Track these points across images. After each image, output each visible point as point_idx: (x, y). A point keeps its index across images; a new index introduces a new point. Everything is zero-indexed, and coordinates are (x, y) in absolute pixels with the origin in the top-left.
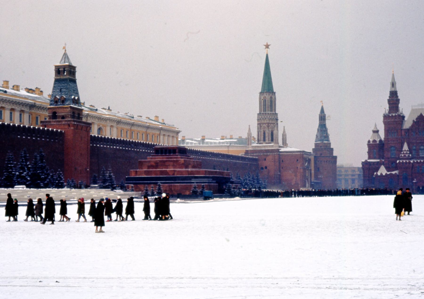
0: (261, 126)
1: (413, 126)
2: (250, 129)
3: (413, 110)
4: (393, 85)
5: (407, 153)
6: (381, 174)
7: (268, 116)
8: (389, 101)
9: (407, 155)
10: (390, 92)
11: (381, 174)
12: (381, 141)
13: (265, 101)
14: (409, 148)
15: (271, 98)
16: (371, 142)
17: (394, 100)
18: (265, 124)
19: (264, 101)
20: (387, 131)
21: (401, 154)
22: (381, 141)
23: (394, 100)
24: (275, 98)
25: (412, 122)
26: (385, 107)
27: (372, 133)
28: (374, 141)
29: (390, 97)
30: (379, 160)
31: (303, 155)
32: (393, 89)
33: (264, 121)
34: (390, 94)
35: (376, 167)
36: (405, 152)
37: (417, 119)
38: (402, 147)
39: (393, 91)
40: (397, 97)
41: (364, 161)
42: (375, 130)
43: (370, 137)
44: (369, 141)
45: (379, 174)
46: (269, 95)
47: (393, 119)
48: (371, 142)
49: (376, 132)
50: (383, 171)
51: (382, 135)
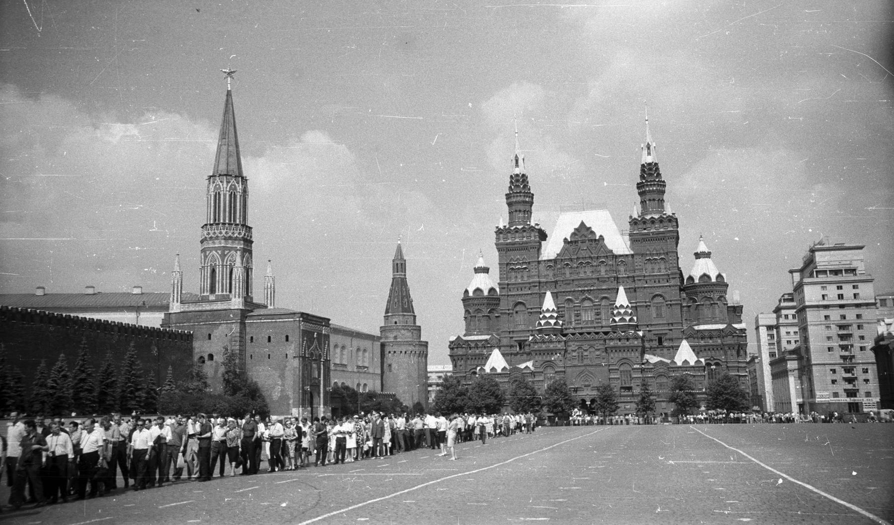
0: (206, 256)
1: (564, 250)
5: (551, 317)
6: (493, 369)
7: (224, 232)
9: (552, 321)
11: (493, 369)
13: (217, 196)
15: (233, 190)
16: (471, 294)
18: (216, 249)
19: (215, 196)
20: (506, 267)
22: (492, 290)
23: (520, 194)
24: (245, 191)
25: (562, 244)
33: (214, 243)
34: (511, 182)
35: (480, 353)
36: (548, 315)
37: (573, 234)
38: (541, 303)
41: (453, 338)
45: (487, 369)
46: (228, 182)
48: (471, 294)
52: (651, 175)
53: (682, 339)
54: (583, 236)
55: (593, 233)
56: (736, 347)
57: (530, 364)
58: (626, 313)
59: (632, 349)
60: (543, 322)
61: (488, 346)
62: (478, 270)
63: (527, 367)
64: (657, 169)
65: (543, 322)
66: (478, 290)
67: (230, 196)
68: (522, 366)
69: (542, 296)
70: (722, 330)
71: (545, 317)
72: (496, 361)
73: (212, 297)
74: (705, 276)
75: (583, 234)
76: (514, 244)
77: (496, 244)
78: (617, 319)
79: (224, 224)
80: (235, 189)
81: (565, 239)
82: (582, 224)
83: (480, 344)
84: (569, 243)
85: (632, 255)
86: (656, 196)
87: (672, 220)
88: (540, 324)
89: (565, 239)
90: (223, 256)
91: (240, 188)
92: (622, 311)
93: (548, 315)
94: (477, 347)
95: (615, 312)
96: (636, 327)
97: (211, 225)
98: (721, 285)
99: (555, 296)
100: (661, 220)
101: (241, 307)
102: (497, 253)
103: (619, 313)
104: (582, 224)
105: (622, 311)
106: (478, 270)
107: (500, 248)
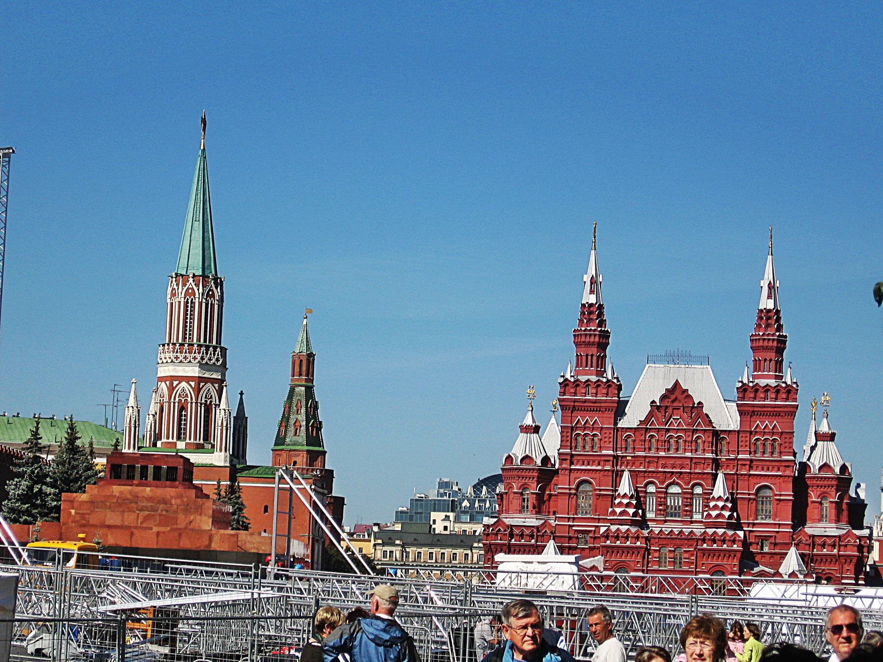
1: (650, 415)
5: (628, 505)
9: (631, 511)
12: (546, 460)
21: (612, 505)
22: (546, 460)
30: (533, 522)
36: (625, 501)
37: (663, 398)
38: (616, 484)
53: (788, 546)
54: (676, 398)
55: (690, 397)
56: (854, 560)
59: (729, 553)
60: (618, 510)
62: (526, 429)
63: (594, 568)
65: (618, 510)
66: (526, 458)
71: (620, 504)
75: (676, 398)
76: (586, 401)
77: (560, 400)
79: (182, 345)
81: (653, 402)
82: (677, 384)
83: (527, 532)
84: (658, 407)
85: (738, 432)
87: (790, 392)
88: (614, 513)
89: (653, 402)
91: (199, 291)
93: (625, 501)
94: (522, 536)
95: (712, 504)
98: (843, 481)
100: (777, 390)
104: (677, 384)
106: (526, 429)
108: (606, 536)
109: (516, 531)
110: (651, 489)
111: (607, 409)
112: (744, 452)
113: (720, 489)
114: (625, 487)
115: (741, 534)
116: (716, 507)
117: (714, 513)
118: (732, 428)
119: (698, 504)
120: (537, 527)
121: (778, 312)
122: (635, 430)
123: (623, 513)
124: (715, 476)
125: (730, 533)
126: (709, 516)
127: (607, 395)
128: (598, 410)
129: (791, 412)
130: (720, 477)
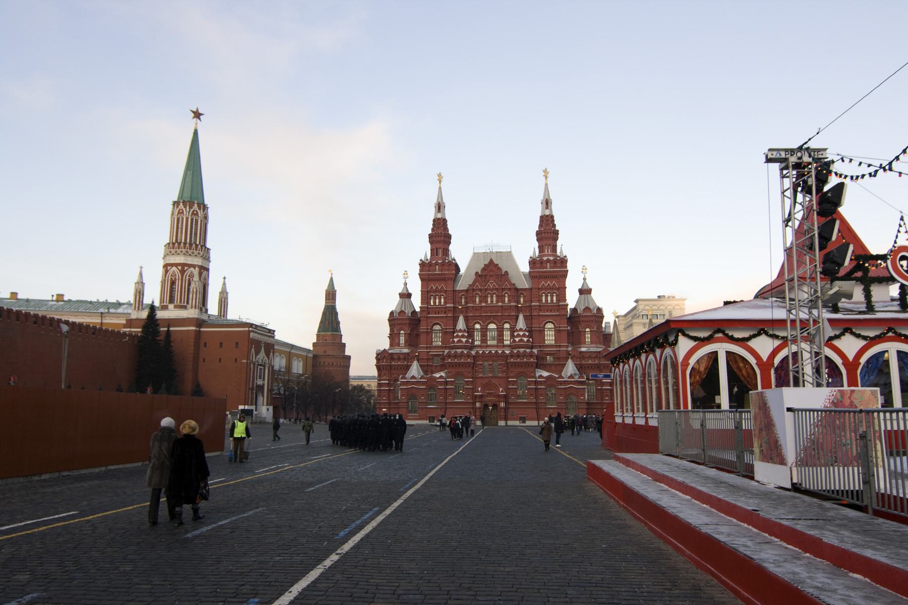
0: (167, 271)
2: (141, 274)
3: (476, 255)
4: (440, 207)
5: (463, 336)
6: (413, 377)
8: (431, 236)
9: (464, 340)
10: (434, 220)
12: (414, 312)
14: (467, 326)
15: (195, 214)
17: (440, 236)
18: (176, 265)
19: (178, 219)
21: (454, 337)
23: (440, 236)
24: (206, 217)
25: (473, 277)
26: (424, 250)
27: (398, 298)
28: (402, 312)
29: (433, 230)
30: (406, 351)
31: (249, 332)
32: (439, 216)
34: (434, 225)
36: (460, 334)
37: (484, 269)
38: (455, 325)
39: (439, 219)
40: (446, 229)
42: (405, 292)
43: (393, 303)
44: (392, 313)
47: (438, 270)
49: (406, 296)
50: (415, 370)
51: (417, 302)
52: (547, 225)
53: (567, 359)
55: (500, 269)
57: (443, 374)
58: (524, 335)
59: (528, 364)
61: (409, 358)
63: (441, 377)
64: (553, 221)
65: (456, 340)
67: (192, 220)
68: (437, 375)
69: (455, 320)
70: (599, 352)
72: (415, 370)
73: (171, 306)
74: (587, 309)
78: (517, 339)
80: (197, 214)
83: (402, 357)
86: (550, 242)
88: (453, 342)
90: (183, 272)
92: (521, 333)
94: (399, 359)
96: (532, 348)
97: (174, 244)
99: (466, 319)
100: (555, 262)
101: (196, 316)
102: (420, 282)
103: (518, 336)
104: (491, 261)
105: (521, 333)
107: (423, 278)
108: (449, 356)
109: (395, 357)
110: (477, 326)
111: (450, 279)
112: (535, 301)
113: (521, 324)
114: (461, 324)
115: (535, 351)
116: (518, 336)
117: (517, 339)
118: (527, 287)
119: (507, 335)
120: (408, 354)
121: (552, 217)
122: (467, 291)
123: (458, 342)
124: (518, 316)
125: (528, 351)
126: (514, 341)
127: (448, 270)
128: (444, 280)
129: (564, 275)
130: (521, 317)
